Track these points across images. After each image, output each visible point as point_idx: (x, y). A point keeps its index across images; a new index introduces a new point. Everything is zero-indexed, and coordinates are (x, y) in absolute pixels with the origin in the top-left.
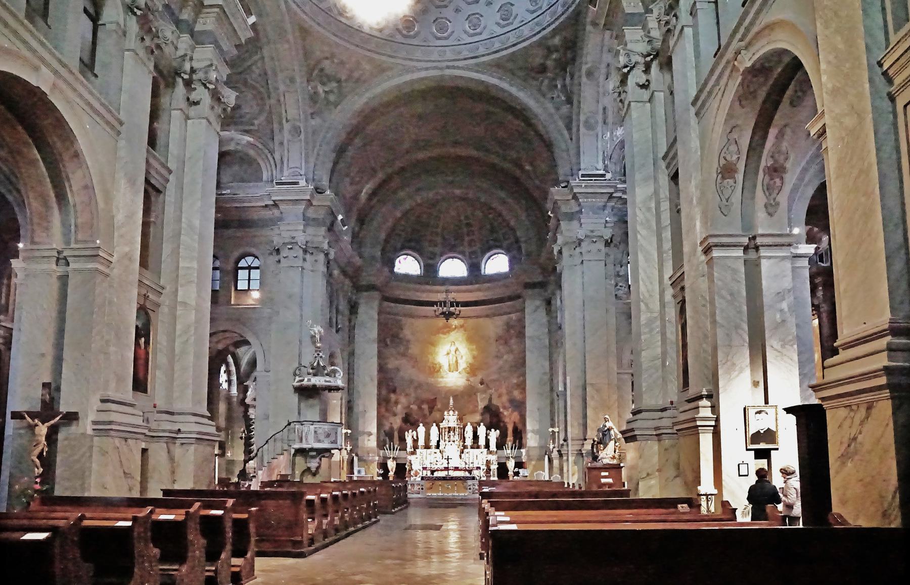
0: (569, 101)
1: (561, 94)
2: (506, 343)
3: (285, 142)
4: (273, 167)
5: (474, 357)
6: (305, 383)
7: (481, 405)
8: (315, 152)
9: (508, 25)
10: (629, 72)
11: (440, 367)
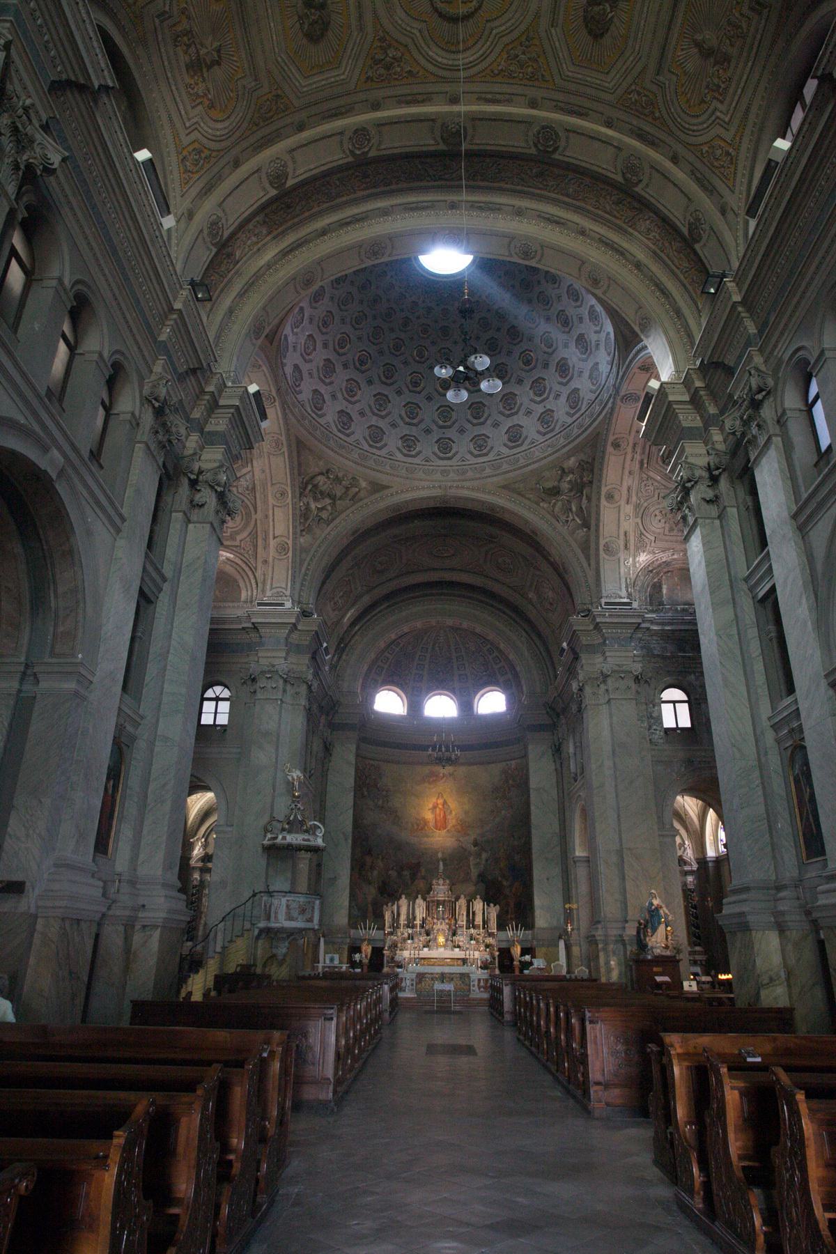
0: (586, 524)
1: (576, 518)
3: (271, 559)
4: (254, 586)
5: (466, 813)
6: (279, 840)
7: (474, 873)
8: (303, 570)
9: (518, 446)
10: (693, 486)
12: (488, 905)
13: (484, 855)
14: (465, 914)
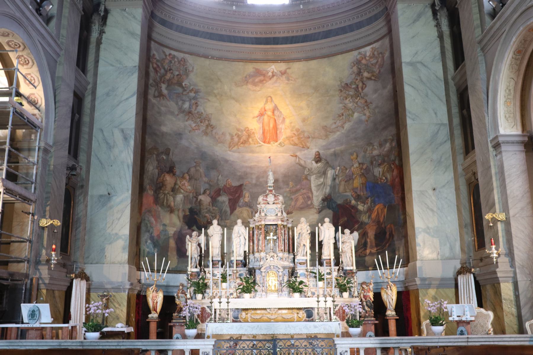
2: (357, 94)
5: (304, 120)
7: (317, 197)
11: (249, 136)
12: (343, 233)
13: (330, 173)
14: (308, 245)
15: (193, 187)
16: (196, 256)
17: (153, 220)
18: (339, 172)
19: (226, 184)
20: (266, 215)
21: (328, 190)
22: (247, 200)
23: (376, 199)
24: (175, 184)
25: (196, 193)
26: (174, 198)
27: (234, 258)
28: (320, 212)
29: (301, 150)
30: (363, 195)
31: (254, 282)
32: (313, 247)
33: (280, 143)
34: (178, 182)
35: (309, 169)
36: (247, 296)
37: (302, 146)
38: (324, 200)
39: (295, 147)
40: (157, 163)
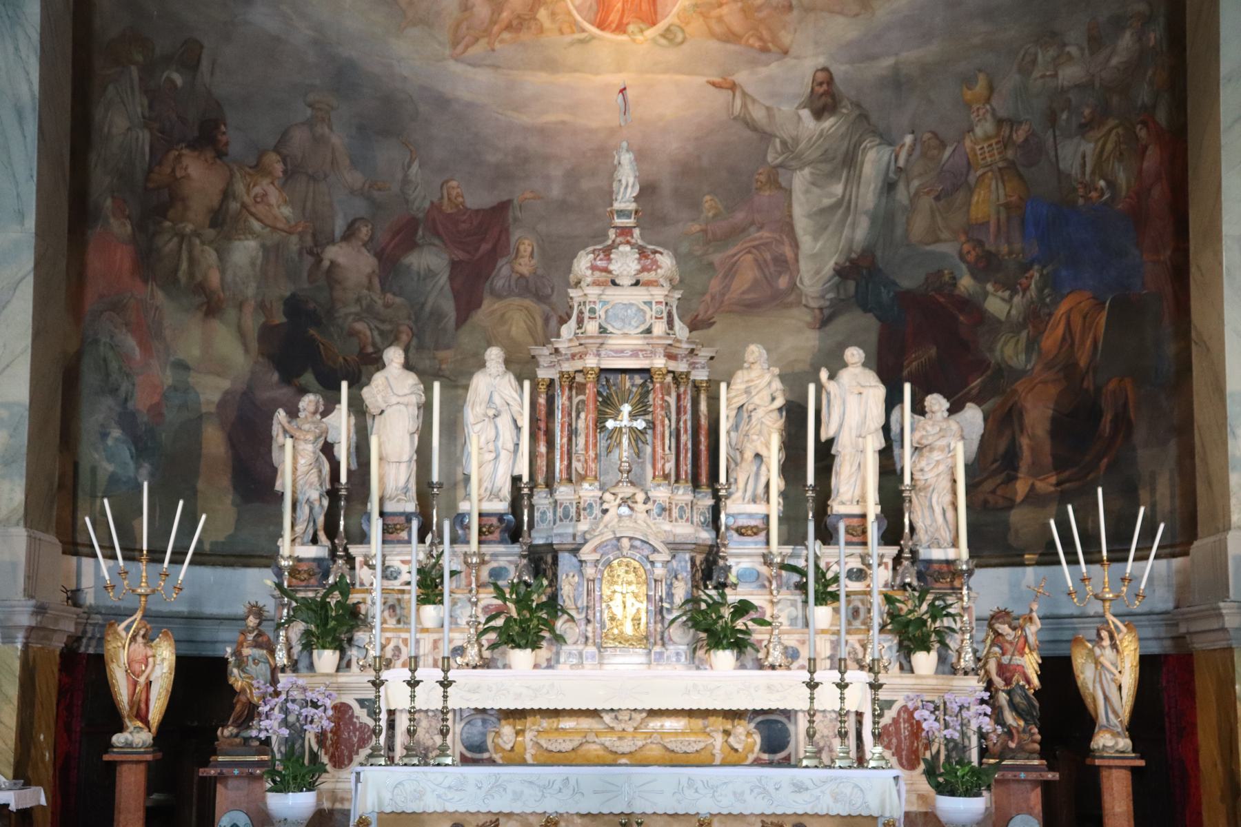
12: (919, 409)
13: (874, 160)
14: (774, 457)
15: (304, 209)
16: (314, 495)
17: (130, 343)
18: (910, 155)
19: (442, 198)
20: (603, 330)
21: (861, 232)
22: (525, 266)
23: (1064, 273)
24: (227, 194)
25: (314, 235)
26: (222, 255)
27: (470, 506)
28: (825, 321)
29: (753, 63)
30: (1010, 253)
31: (553, 605)
32: (792, 466)
33: (668, 30)
34: (240, 187)
35: (784, 143)
36: (521, 658)
37: (757, 44)
38: (842, 273)
39: (731, 47)
40: (146, 102)
